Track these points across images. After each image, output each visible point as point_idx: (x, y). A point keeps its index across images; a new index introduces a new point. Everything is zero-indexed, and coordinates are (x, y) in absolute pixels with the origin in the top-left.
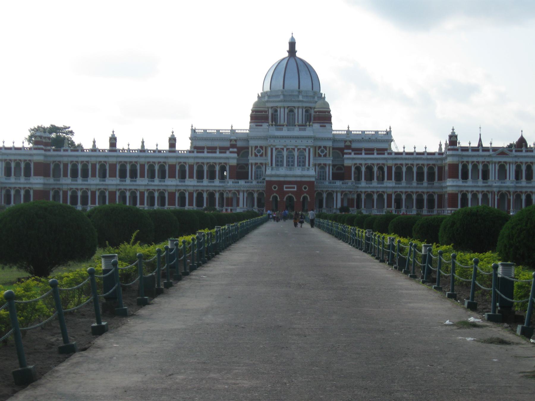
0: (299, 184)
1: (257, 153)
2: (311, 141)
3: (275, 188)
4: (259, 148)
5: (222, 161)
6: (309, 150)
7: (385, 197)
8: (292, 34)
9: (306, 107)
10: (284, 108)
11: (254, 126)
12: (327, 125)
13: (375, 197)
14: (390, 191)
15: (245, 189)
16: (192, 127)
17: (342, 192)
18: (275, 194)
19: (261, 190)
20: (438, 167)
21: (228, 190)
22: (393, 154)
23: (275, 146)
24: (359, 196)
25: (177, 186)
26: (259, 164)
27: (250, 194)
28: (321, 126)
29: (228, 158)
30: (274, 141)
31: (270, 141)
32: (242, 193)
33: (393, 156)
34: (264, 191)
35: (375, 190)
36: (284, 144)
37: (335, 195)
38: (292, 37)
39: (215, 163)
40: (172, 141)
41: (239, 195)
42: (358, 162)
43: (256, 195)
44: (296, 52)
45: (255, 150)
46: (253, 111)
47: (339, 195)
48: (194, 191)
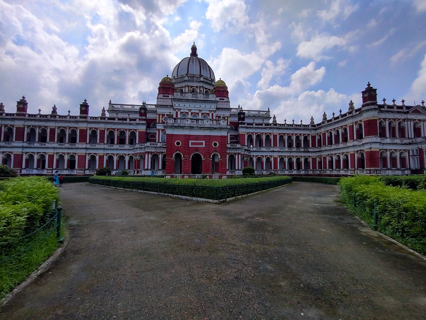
0: (209, 139)
1: (163, 120)
2: (215, 107)
3: (178, 144)
4: (166, 116)
6: (213, 114)
7: (272, 160)
8: (194, 43)
9: (206, 89)
11: (162, 97)
12: (226, 99)
13: (264, 160)
16: (110, 102)
17: (242, 155)
18: (178, 152)
20: (312, 136)
22: (278, 125)
23: (180, 110)
24: (251, 159)
25: (86, 149)
27: (155, 157)
28: (220, 99)
30: (179, 105)
33: (278, 126)
36: (188, 108)
38: (194, 44)
39: (126, 130)
40: (84, 108)
44: (197, 55)
45: (162, 118)
47: (240, 156)
48: (104, 154)
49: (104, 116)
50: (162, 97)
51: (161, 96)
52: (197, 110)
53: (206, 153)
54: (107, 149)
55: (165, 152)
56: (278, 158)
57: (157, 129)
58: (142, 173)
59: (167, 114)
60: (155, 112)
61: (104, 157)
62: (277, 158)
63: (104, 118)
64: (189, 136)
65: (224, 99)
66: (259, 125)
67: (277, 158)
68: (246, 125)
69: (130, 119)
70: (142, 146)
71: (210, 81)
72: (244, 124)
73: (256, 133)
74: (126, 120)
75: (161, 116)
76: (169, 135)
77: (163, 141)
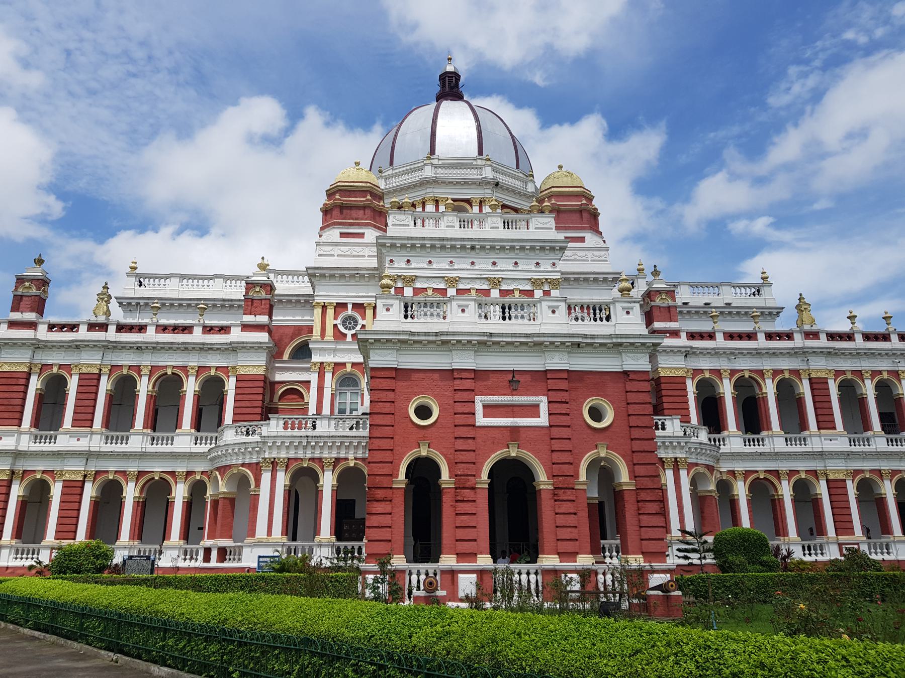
3: (423, 412)
4: (350, 311)
5: (214, 361)
10: (437, 201)
11: (337, 239)
13: (786, 490)
14: (836, 467)
15: (283, 455)
19: (352, 457)
21: (218, 469)
24: (724, 487)
26: (349, 368)
29: (234, 348)
31: (391, 261)
32: (270, 474)
33: (823, 342)
34: (363, 460)
35: (783, 466)
37: (668, 477)
41: (258, 484)
42: (705, 364)
43: (328, 481)
45: (335, 318)
46: (330, 194)
48: (85, 476)
49: (102, 319)
50: (337, 239)
51: (333, 234)
52: (483, 281)
53: (555, 455)
54: (99, 455)
55: (346, 459)
56: (849, 484)
57: (315, 364)
58: (244, 557)
59: (353, 304)
60: (305, 302)
61: (82, 488)
62: (844, 481)
63: (103, 327)
64: (477, 375)
65: (582, 240)
66: (740, 336)
67: (844, 481)
68: (683, 341)
69: (204, 327)
70: (248, 434)
71: (517, 178)
72: (675, 334)
73: (733, 372)
74: (191, 333)
75: (330, 312)
76: (382, 374)
77: (336, 410)
